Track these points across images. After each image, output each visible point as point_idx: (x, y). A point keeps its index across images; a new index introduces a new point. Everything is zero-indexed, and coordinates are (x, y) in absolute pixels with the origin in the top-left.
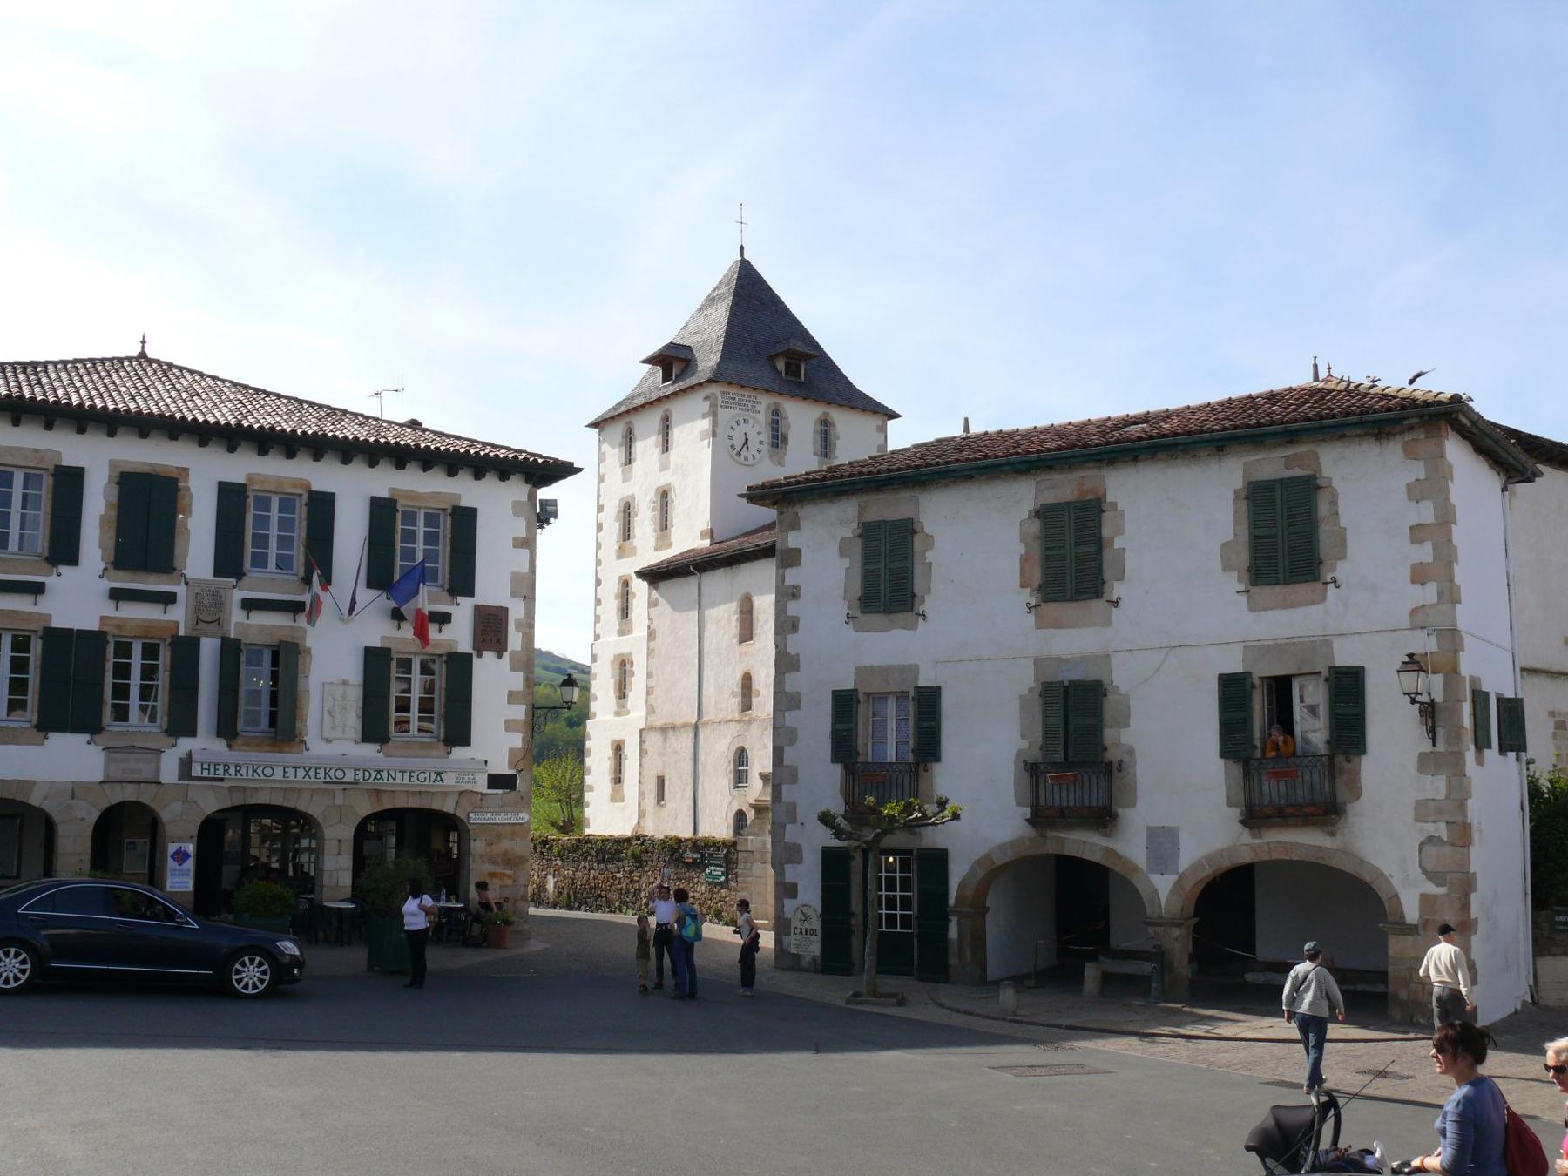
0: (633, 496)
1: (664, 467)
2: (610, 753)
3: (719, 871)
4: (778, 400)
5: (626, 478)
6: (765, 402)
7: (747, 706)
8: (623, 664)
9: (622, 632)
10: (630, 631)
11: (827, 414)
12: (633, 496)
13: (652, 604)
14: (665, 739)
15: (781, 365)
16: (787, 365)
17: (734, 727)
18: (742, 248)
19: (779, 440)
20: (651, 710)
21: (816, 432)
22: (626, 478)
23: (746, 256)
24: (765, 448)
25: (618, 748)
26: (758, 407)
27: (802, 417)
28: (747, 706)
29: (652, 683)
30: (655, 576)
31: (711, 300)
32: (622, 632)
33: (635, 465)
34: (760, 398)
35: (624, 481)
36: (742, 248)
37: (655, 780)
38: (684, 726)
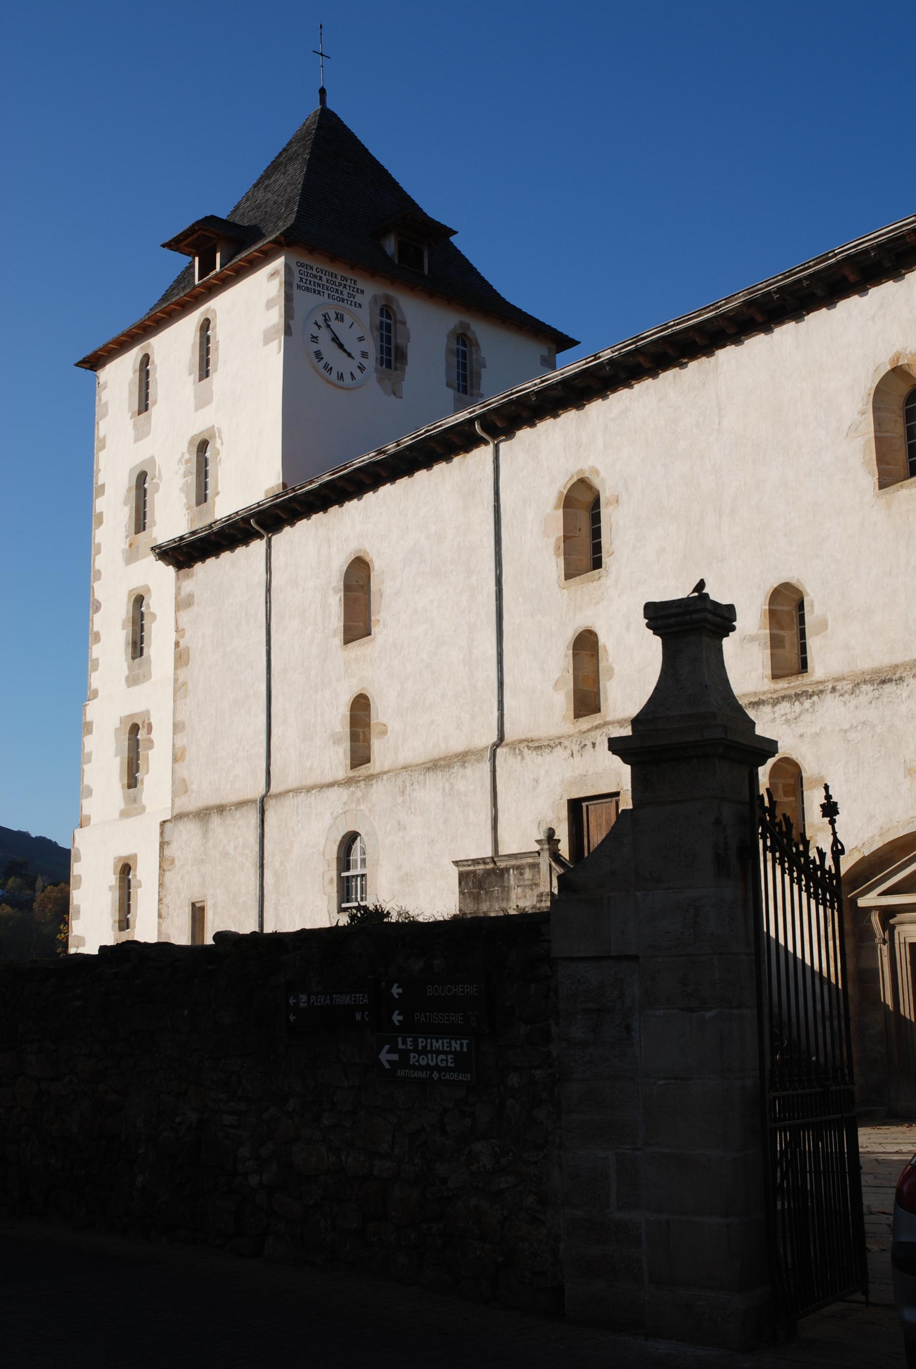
0: (152, 460)
1: (202, 401)
2: (112, 879)
3: (440, 1053)
4: (391, 292)
5: (141, 434)
6: (370, 291)
7: (360, 756)
8: (135, 729)
9: (133, 680)
10: (147, 676)
11: (465, 326)
12: (152, 460)
13: (183, 603)
14: (206, 832)
15: (391, 246)
16: (402, 247)
17: (338, 797)
18: (322, 91)
19: (392, 356)
20: (180, 787)
21: (449, 351)
22: (141, 434)
23: (330, 105)
24: (371, 363)
25: (125, 870)
26: (359, 298)
27: (428, 327)
28: (360, 756)
29: (182, 741)
30: (184, 554)
31: (275, 167)
32: (133, 680)
33: (154, 410)
34: (360, 285)
35: (137, 439)
36: (322, 91)
37: (188, 910)
38: (241, 804)
